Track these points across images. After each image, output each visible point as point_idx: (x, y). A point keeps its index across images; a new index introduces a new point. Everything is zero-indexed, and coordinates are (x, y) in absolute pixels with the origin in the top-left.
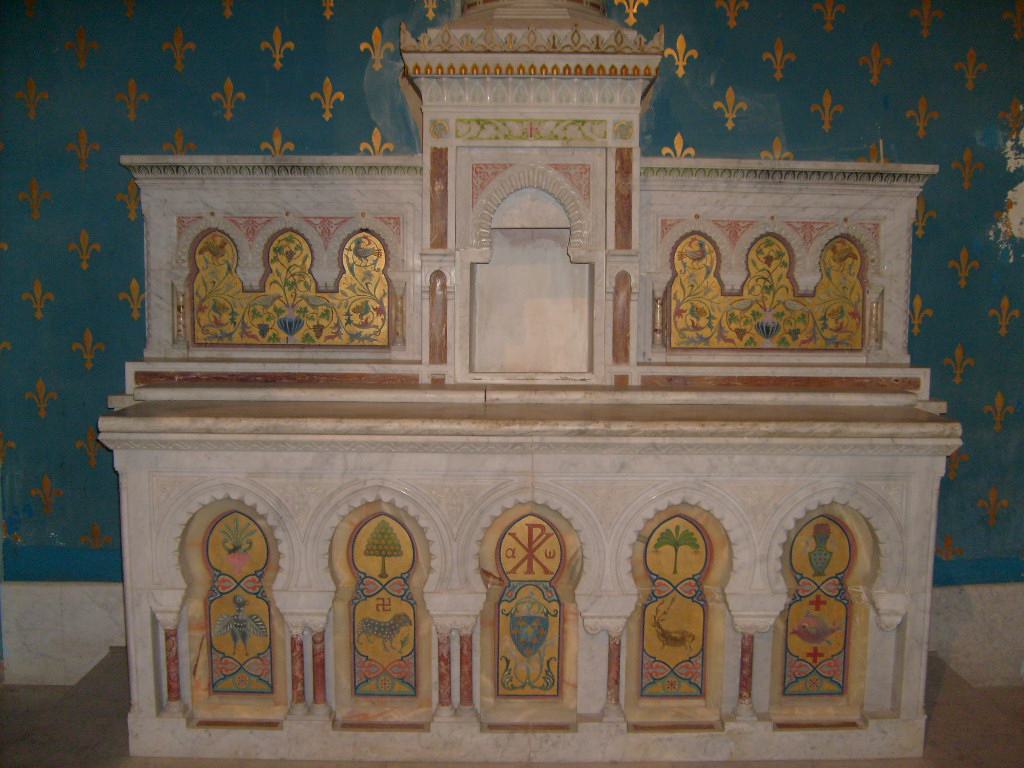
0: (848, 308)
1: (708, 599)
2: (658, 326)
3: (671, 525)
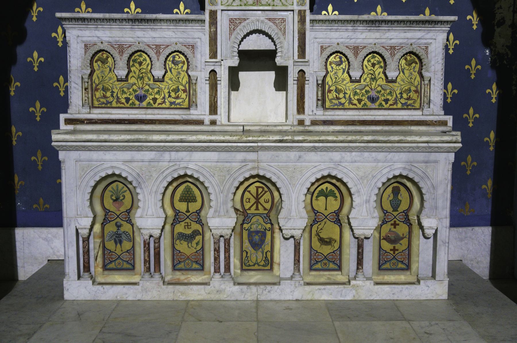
0: (413, 88)
1: (342, 222)
2: (320, 98)
3: (324, 187)
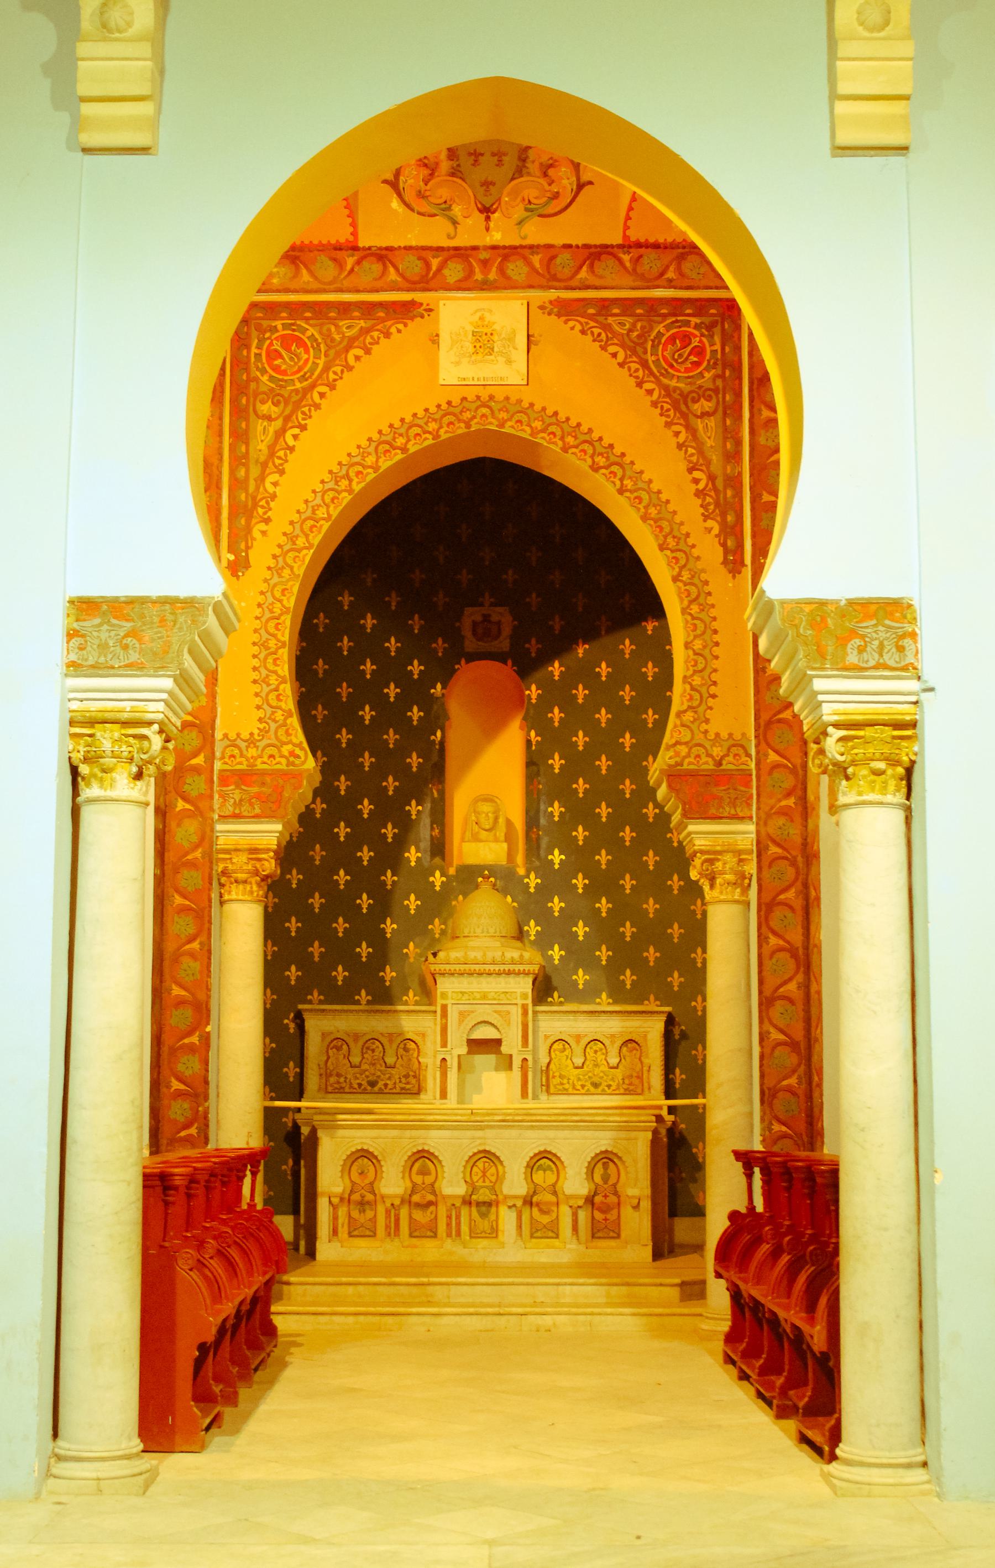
0: (635, 1074)
